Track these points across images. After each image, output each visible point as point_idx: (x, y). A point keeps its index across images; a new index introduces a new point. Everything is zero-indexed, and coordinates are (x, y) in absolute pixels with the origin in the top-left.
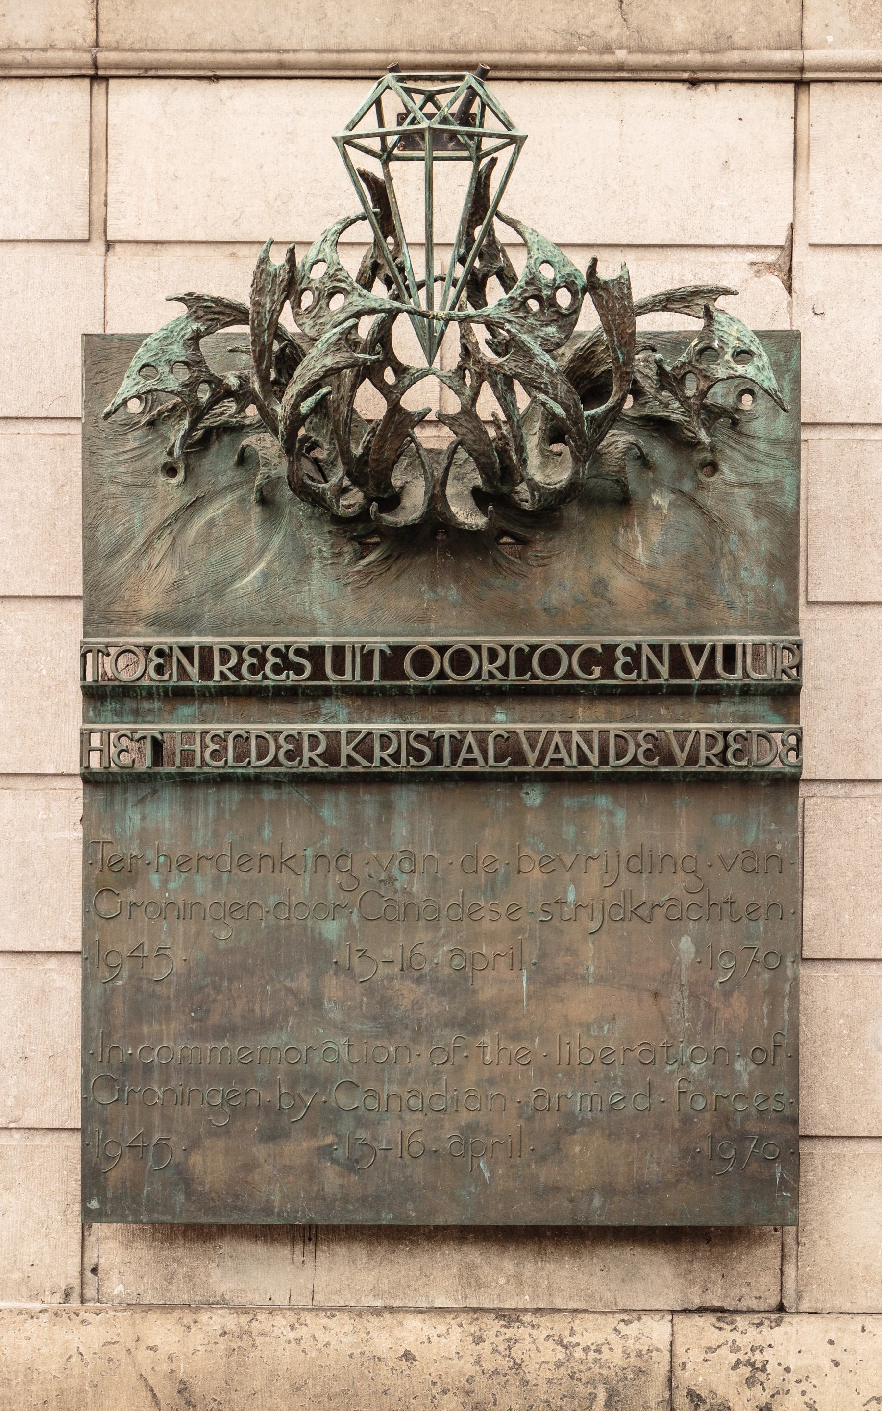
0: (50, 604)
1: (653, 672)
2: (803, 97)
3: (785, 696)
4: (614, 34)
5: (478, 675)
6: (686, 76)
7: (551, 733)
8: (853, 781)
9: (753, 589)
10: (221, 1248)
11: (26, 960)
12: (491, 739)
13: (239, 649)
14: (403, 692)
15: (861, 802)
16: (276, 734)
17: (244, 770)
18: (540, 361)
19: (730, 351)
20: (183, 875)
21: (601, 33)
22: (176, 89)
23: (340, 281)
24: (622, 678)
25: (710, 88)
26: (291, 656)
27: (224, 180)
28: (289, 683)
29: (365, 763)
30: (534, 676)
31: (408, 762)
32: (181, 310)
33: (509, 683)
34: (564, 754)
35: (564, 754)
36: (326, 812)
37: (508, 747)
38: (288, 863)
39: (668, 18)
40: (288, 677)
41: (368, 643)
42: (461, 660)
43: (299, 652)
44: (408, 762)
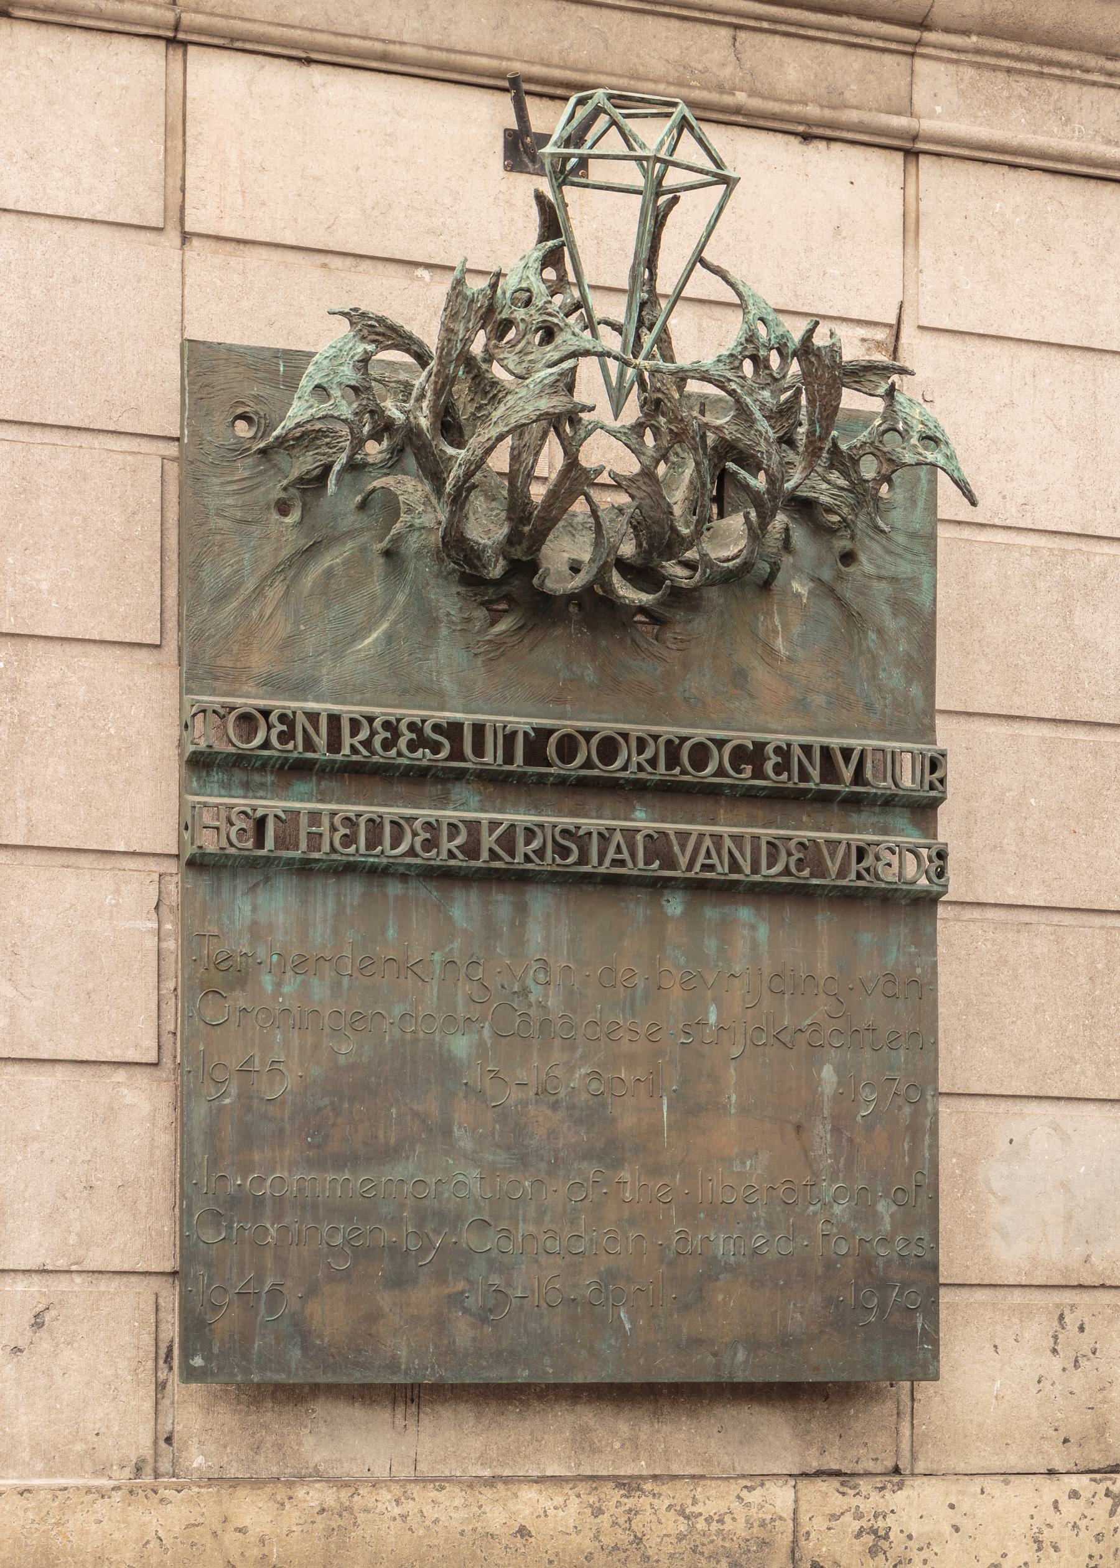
0: (118, 651)
1: (804, 776)
2: (912, 169)
3: (924, 809)
4: (728, 71)
5: (625, 768)
6: (801, 129)
7: (701, 835)
8: (962, 903)
9: (892, 691)
10: (314, 1411)
11: (89, 1071)
12: (639, 837)
13: (371, 720)
14: (542, 779)
15: (972, 927)
16: (411, 820)
17: (376, 860)
18: (760, 428)
19: (916, 436)
20: (299, 978)
21: (715, 69)
22: (263, 67)
23: (550, 315)
24: (772, 779)
25: (822, 145)
26: (428, 729)
27: (316, 179)
28: (425, 762)
29: (508, 859)
30: (684, 772)
31: (554, 859)
32: (343, 327)
33: (658, 778)
34: (715, 860)
35: (715, 860)
36: (457, 912)
37: (658, 847)
38: (414, 968)
39: (780, 64)
40: (424, 756)
41: (510, 722)
42: (608, 748)
43: (436, 728)
44: (554, 859)
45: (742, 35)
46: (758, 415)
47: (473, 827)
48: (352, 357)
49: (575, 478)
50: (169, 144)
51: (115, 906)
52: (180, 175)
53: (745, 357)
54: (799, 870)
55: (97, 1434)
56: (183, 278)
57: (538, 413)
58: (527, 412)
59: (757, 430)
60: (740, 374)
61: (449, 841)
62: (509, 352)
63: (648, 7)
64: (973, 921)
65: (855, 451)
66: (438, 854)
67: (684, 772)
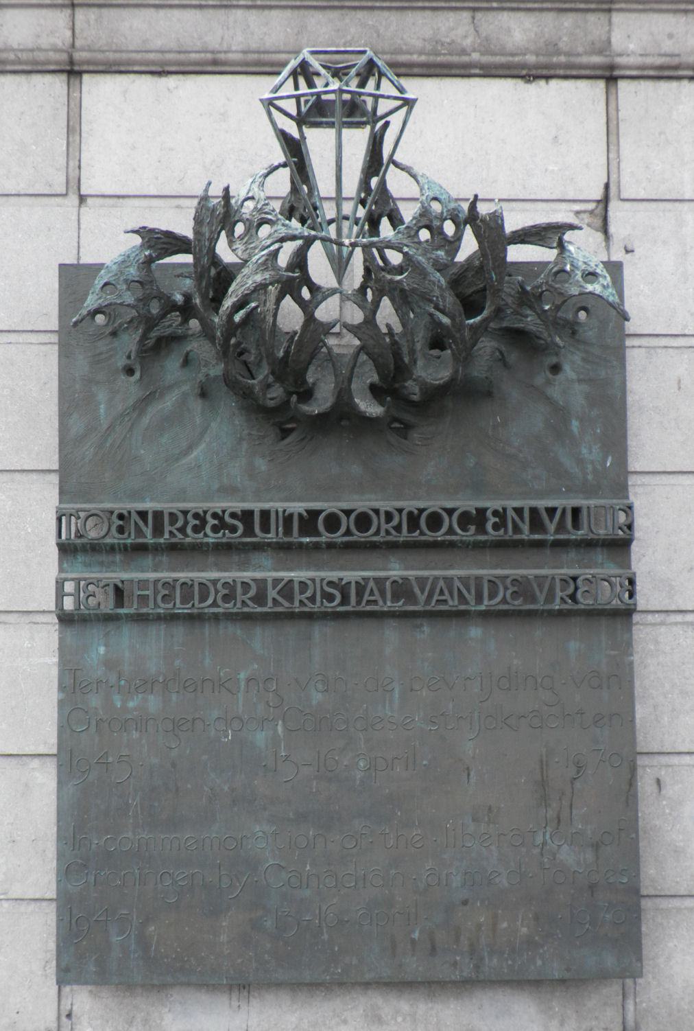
0: (34, 476)
1: (517, 529)
2: (613, 90)
3: (620, 546)
4: (468, 42)
5: (377, 533)
6: (524, 72)
7: (436, 579)
8: (667, 611)
9: (592, 462)
10: (171, 995)
11: (14, 761)
12: (388, 584)
13: (185, 513)
14: (317, 547)
15: (675, 629)
16: (215, 582)
17: (189, 611)
18: (433, 279)
19: (579, 274)
20: (140, 696)
21: (459, 41)
22: (134, 81)
23: (266, 213)
24: (492, 534)
25: (542, 83)
26: (227, 518)
27: (172, 149)
28: (224, 540)
29: (286, 604)
30: (422, 533)
31: (322, 602)
32: (137, 240)
33: (402, 539)
34: (447, 596)
35: (447, 596)
36: (257, 645)
37: (402, 590)
38: (226, 685)
39: (509, 30)
40: (224, 534)
41: (288, 507)
42: (363, 521)
43: (233, 515)
44: (322, 602)
45: (479, 15)
46: (430, 269)
47: (262, 583)
48: (138, 261)
49: (314, 329)
50: (71, 139)
51: (31, 648)
52: (78, 158)
53: (421, 228)
54: (513, 599)
55: (18, 1013)
56: (79, 225)
57: (254, 285)
58: (248, 285)
59: (430, 281)
60: (416, 240)
61: (244, 594)
62: (240, 244)
63: (406, 4)
64: (676, 624)
65: (536, 290)
66: (235, 605)
67: (422, 533)
